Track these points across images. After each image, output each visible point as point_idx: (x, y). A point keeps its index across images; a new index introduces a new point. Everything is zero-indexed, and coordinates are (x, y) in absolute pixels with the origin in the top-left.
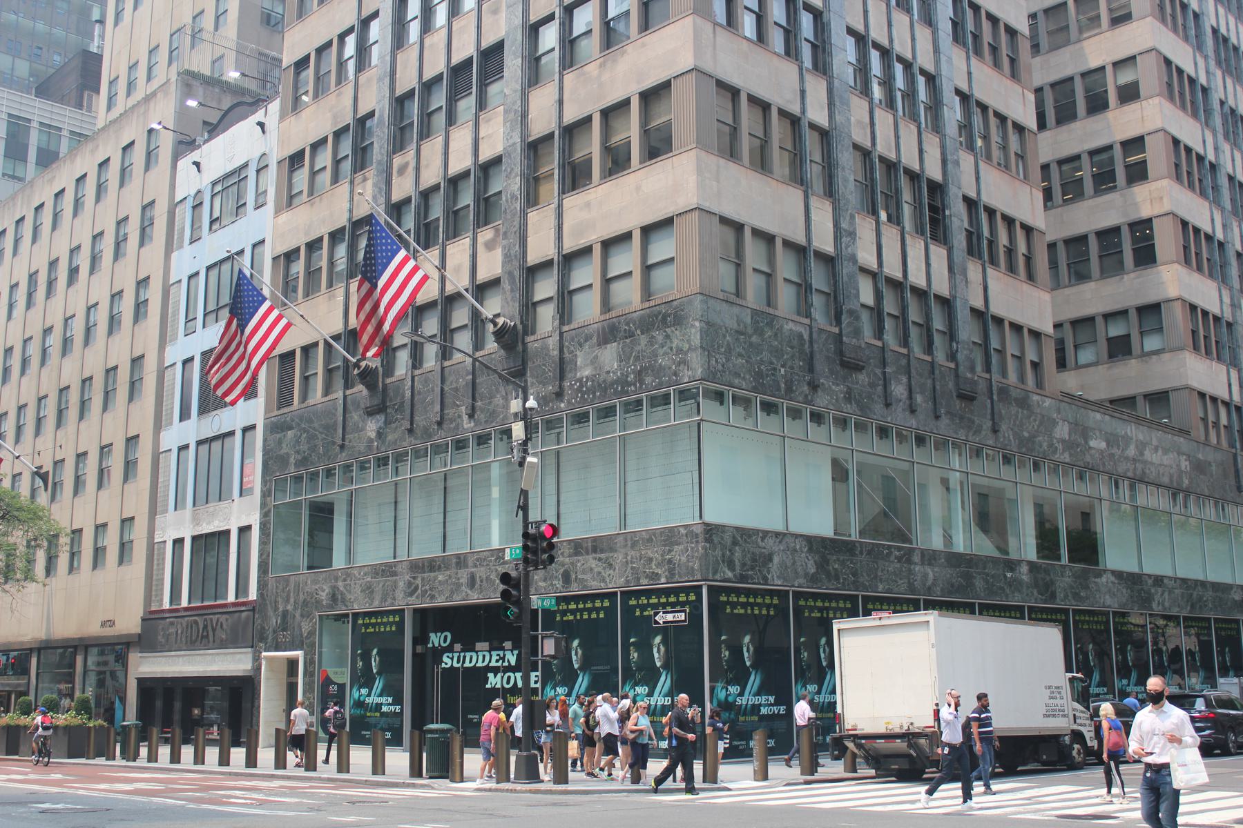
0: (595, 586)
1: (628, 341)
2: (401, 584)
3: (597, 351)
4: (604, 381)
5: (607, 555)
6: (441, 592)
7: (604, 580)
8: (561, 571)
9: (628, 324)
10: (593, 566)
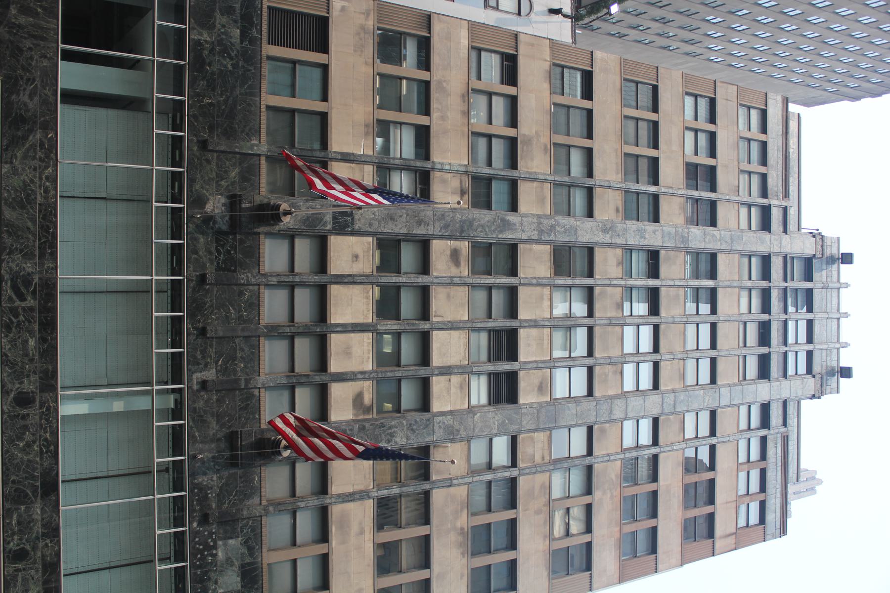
2: (29, 267)
3: (236, 568)
4: (209, 579)
6: (13, 342)
8: (28, 547)
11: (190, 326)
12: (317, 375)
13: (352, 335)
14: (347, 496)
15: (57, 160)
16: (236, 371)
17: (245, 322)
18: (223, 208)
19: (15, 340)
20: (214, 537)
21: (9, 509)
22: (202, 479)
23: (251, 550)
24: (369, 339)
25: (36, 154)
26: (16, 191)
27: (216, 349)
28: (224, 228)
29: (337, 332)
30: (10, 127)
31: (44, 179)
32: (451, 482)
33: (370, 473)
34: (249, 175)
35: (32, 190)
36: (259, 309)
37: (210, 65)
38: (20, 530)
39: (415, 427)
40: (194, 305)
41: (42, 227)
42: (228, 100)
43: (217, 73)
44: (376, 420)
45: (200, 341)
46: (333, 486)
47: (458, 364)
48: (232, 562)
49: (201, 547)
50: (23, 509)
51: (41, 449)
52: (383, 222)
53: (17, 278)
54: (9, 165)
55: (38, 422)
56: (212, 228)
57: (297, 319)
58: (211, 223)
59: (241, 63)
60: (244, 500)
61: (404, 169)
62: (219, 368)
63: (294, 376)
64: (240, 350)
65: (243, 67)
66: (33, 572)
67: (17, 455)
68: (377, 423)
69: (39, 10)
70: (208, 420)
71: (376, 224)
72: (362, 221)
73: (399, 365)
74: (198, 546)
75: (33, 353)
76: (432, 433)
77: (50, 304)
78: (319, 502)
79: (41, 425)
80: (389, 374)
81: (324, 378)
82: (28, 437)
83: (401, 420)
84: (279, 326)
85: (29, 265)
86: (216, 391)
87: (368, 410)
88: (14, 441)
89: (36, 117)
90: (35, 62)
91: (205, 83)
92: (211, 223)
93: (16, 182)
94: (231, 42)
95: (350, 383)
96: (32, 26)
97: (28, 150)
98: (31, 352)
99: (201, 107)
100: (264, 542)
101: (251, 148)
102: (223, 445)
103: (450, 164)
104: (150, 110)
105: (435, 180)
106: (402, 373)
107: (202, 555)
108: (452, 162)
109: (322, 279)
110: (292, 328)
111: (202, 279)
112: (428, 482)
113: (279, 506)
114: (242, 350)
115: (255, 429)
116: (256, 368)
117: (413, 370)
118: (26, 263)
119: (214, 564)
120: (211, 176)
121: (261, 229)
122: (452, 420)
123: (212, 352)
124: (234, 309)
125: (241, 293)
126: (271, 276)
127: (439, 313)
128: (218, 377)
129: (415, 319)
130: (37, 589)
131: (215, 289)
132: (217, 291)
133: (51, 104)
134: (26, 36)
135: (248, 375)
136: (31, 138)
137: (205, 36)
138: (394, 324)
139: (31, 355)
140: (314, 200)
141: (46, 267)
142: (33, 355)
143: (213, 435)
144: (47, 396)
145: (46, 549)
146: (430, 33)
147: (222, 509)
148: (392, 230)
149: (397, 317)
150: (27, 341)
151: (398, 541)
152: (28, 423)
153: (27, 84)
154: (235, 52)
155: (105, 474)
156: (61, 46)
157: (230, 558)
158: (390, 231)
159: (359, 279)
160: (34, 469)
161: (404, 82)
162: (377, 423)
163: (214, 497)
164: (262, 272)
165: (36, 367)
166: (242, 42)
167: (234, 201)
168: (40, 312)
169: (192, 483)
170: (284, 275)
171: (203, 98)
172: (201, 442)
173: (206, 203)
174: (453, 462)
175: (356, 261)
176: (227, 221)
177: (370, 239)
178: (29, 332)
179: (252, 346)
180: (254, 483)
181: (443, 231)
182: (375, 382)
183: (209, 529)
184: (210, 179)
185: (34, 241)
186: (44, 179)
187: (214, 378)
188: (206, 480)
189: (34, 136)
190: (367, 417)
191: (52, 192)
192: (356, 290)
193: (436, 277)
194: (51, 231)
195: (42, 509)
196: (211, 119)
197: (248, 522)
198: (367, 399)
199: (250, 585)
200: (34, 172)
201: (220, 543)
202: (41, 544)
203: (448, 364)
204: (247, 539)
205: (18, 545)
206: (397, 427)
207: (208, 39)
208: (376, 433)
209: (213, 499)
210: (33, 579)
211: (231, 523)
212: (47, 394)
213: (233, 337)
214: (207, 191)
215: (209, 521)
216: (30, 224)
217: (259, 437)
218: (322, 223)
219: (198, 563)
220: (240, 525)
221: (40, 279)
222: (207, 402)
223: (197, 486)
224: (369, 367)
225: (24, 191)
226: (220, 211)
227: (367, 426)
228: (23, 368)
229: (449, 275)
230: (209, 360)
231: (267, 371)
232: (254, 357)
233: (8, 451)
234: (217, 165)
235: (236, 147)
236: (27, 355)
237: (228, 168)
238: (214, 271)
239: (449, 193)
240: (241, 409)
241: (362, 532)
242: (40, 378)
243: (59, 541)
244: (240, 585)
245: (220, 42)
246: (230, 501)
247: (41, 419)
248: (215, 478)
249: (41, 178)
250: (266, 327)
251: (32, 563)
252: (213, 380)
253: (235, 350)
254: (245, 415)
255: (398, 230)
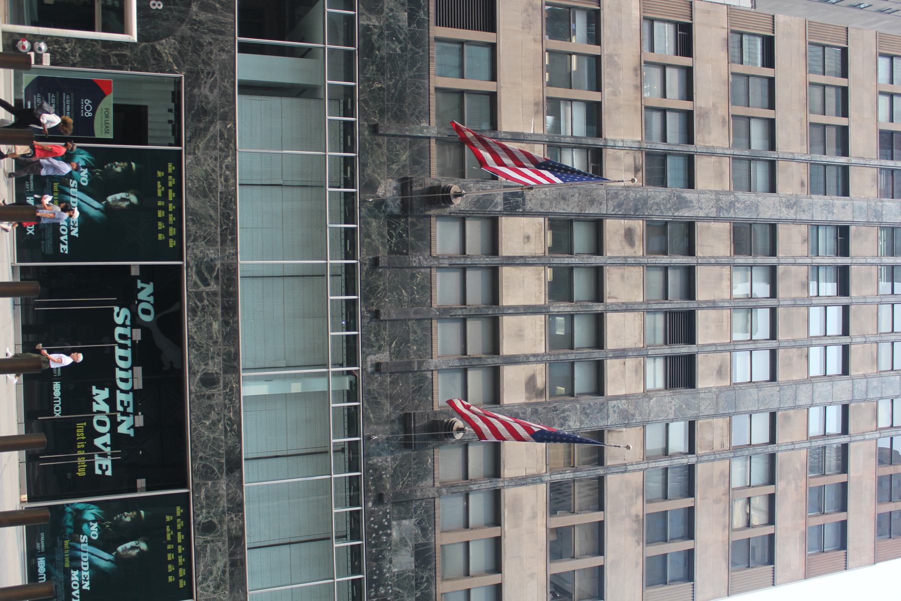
0: (198, 568)
1: (413, 583)
2: (211, 253)
3: (410, 548)
4: (384, 557)
5: (228, 581)
6: (198, 325)
7: (205, 579)
8: (215, 521)
9: (428, 580)
10: (218, 564)
11: (364, 309)
12: (490, 358)
13: (525, 317)
14: (520, 480)
15: (236, 149)
16: (410, 353)
17: (417, 304)
18: (395, 192)
19: (200, 323)
20: (388, 517)
21: (198, 484)
22: (375, 460)
23: (424, 530)
24: (541, 321)
25: (216, 144)
26: (199, 180)
27: (389, 331)
28: (396, 211)
29: (510, 314)
30: (192, 120)
31: (224, 168)
32: (626, 468)
33: (543, 457)
34: (419, 158)
35: (214, 180)
36: (431, 292)
37: (379, 50)
38: (208, 504)
39: (588, 411)
40: (368, 288)
41: (223, 215)
42: (397, 84)
43: (386, 56)
44: (549, 403)
45: (373, 324)
46: (506, 469)
47: (633, 347)
48: (406, 542)
49: (376, 526)
50: (210, 484)
51: (225, 428)
52: (555, 202)
53: (201, 264)
54: (192, 156)
55: (222, 402)
56: (384, 212)
57: (469, 302)
58: (383, 207)
59: (409, 46)
60: (417, 482)
61: (575, 147)
62: (392, 350)
63: (467, 359)
64: (412, 332)
65: (411, 50)
66: (220, 544)
67: (204, 433)
68: (549, 406)
69: (218, 6)
70: (382, 402)
71: (547, 204)
72: (534, 201)
73: (572, 348)
74: (373, 525)
75: (217, 336)
76: (606, 417)
77: (231, 289)
78: (491, 485)
79: (225, 405)
80: (562, 357)
81: (494, 359)
82: (213, 416)
83: (574, 404)
84: (451, 308)
85: (212, 251)
86: (390, 373)
87: (541, 393)
88: (200, 419)
89: (216, 109)
90: (214, 55)
91: (375, 68)
92: (383, 207)
93: (199, 172)
94: (399, 26)
95: (522, 366)
96: (211, 21)
97: (209, 141)
98: (215, 335)
99: (371, 91)
100: (437, 524)
101: (421, 131)
102: (397, 427)
103: (622, 141)
104: (322, 97)
105: (607, 158)
106: (576, 356)
107: (377, 534)
108: (625, 138)
109: (494, 261)
110: (464, 310)
111: (375, 262)
112: (602, 467)
113: (452, 489)
114: (415, 332)
115: (428, 411)
116: (429, 351)
117: (586, 353)
118: (209, 250)
119: (388, 544)
120: (382, 161)
121: (432, 212)
122: (627, 405)
123: (385, 334)
124: (407, 292)
125: (413, 276)
126: (443, 258)
127: (612, 295)
128: (391, 360)
129: (589, 301)
130: (225, 560)
131: (388, 272)
132: (390, 274)
133: (230, 95)
134: (206, 31)
135: (421, 358)
136: (212, 129)
137: (374, 21)
138: (567, 306)
139: (215, 338)
140: (484, 181)
141: (227, 253)
142: (217, 338)
143: (387, 416)
144: (230, 377)
145: (231, 523)
146: (599, 6)
147: (395, 489)
148: (564, 210)
149: (571, 299)
150: (211, 325)
151: (571, 526)
152: (213, 402)
153: (207, 78)
154: (403, 36)
155: (285, 453)
156: (238, 39)
157: (404, 538)
158: (562, 211)
159: (530, 261)
160: (220, 447)
161: (574, 57)
162: (549, 406)
163: (388, 478)
164: (434, 254)
165: (220, 349)
166: (409, 25)
167: (405, 185)
168: (223, 297)
169: (367, 463)
170: (456, 258)
171: (373, 83)
172: (376, 424)
173: (377, 188)
174: (628, 447)
175: (528, 242)
176: (398, 205)
177: (542, 220)
178: (213, 315)
179: (424, 329)
180: (427, 465)
181: (617, 210)
182: (547, 364)
183: (383, 509)
184: (381, 163)
185: (216, 228)
186: (224, 168)
187: (388, 360)
188: (380, 461)
189: (215, 127)
190: (539, 400)
191: (232, 181)
192: (528, 271)
193: (610, 258)
194: (231, 218)
195: (227, 485)
196: (381, 103)
197: (421, 503)
198: (540, 382)
199: (423, 566)
200: (214, 162)
201: (394, 523)
202: (227, 518)
203: (623, 347)
204: (421, 520)
205: (206, 518)
206: (570, 411)
207: (377, 24)
208: (549, 417)
209: (387, 480)
210: (220, 550)
211: (405, 503)
212: (230, 376)
213: (405, 320)
214: (379, 175)
215: (383, 502)
216: (212, 212)
217: (432, 419)
218: (493, 205)
219: (373, 542)
220: (414, 506)
221: (222, 264)
222: (381, 384)
223: (371, 466)
224: (541, 349)
225: (206, 180)
226: (392, 195)
227: (540, 409)
228: (208, 350)
229: (623, 255)
230: (382, 343)
231: (439, 354)
232: (427, 340)
233: (195, 429)
234: (388, 149)
235: (407, 130)
236: (211, 338)
237: (399, 151)
238: (386, 255)
239: (622, 170)
240: (413, 392)
241: (534, 516)
242: (224, 360)
243: (243, 516)
244: (413, 565)
245: (389, 27)
246: (404, 482)
247: (225, 399)
248: (389, 459)
249: (221, 168)
250: (438, 310)
251: (219, 536)
252: (387, 363)
253: (408, 333)
254: (418, 397)
255: (570, 210)
